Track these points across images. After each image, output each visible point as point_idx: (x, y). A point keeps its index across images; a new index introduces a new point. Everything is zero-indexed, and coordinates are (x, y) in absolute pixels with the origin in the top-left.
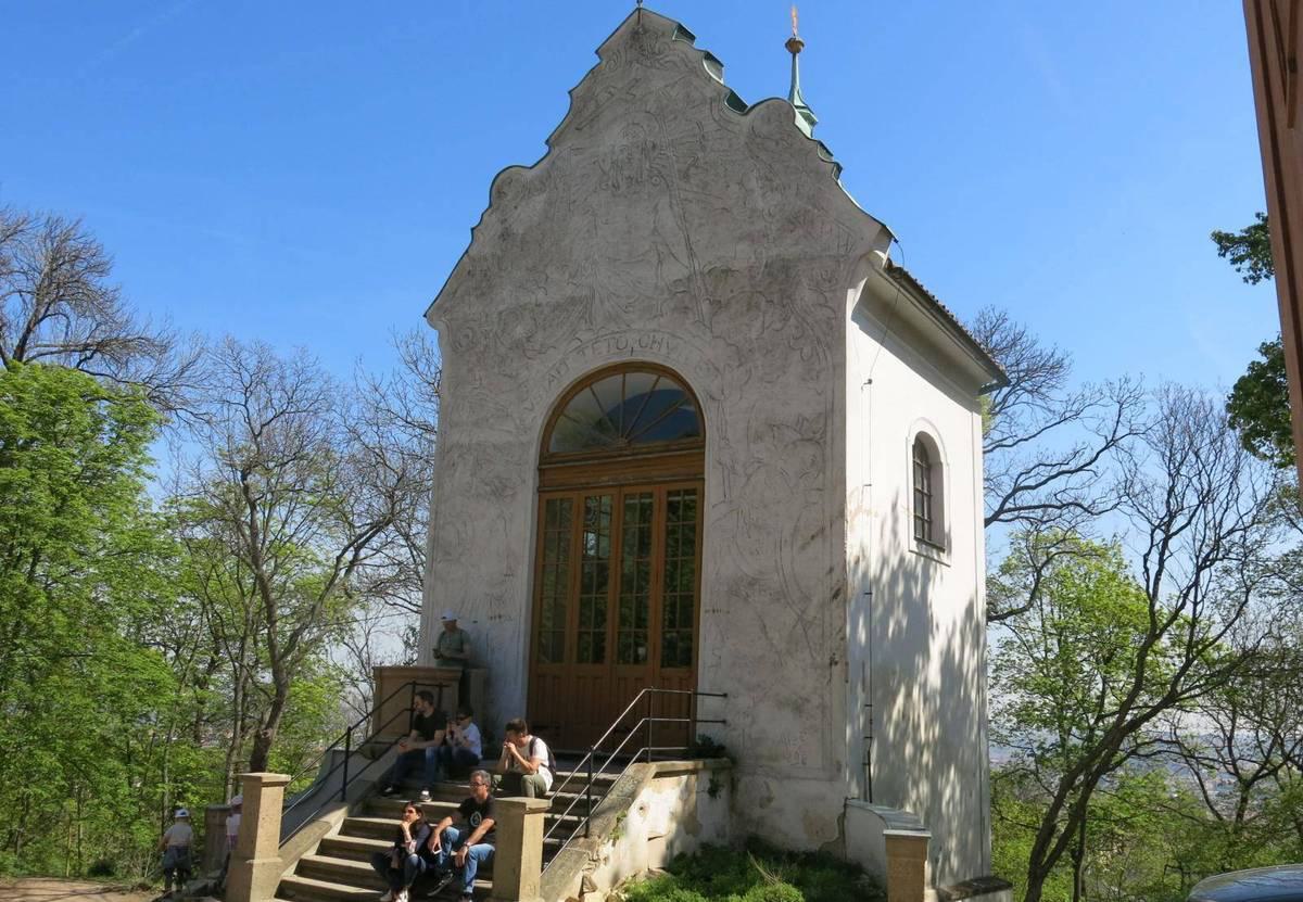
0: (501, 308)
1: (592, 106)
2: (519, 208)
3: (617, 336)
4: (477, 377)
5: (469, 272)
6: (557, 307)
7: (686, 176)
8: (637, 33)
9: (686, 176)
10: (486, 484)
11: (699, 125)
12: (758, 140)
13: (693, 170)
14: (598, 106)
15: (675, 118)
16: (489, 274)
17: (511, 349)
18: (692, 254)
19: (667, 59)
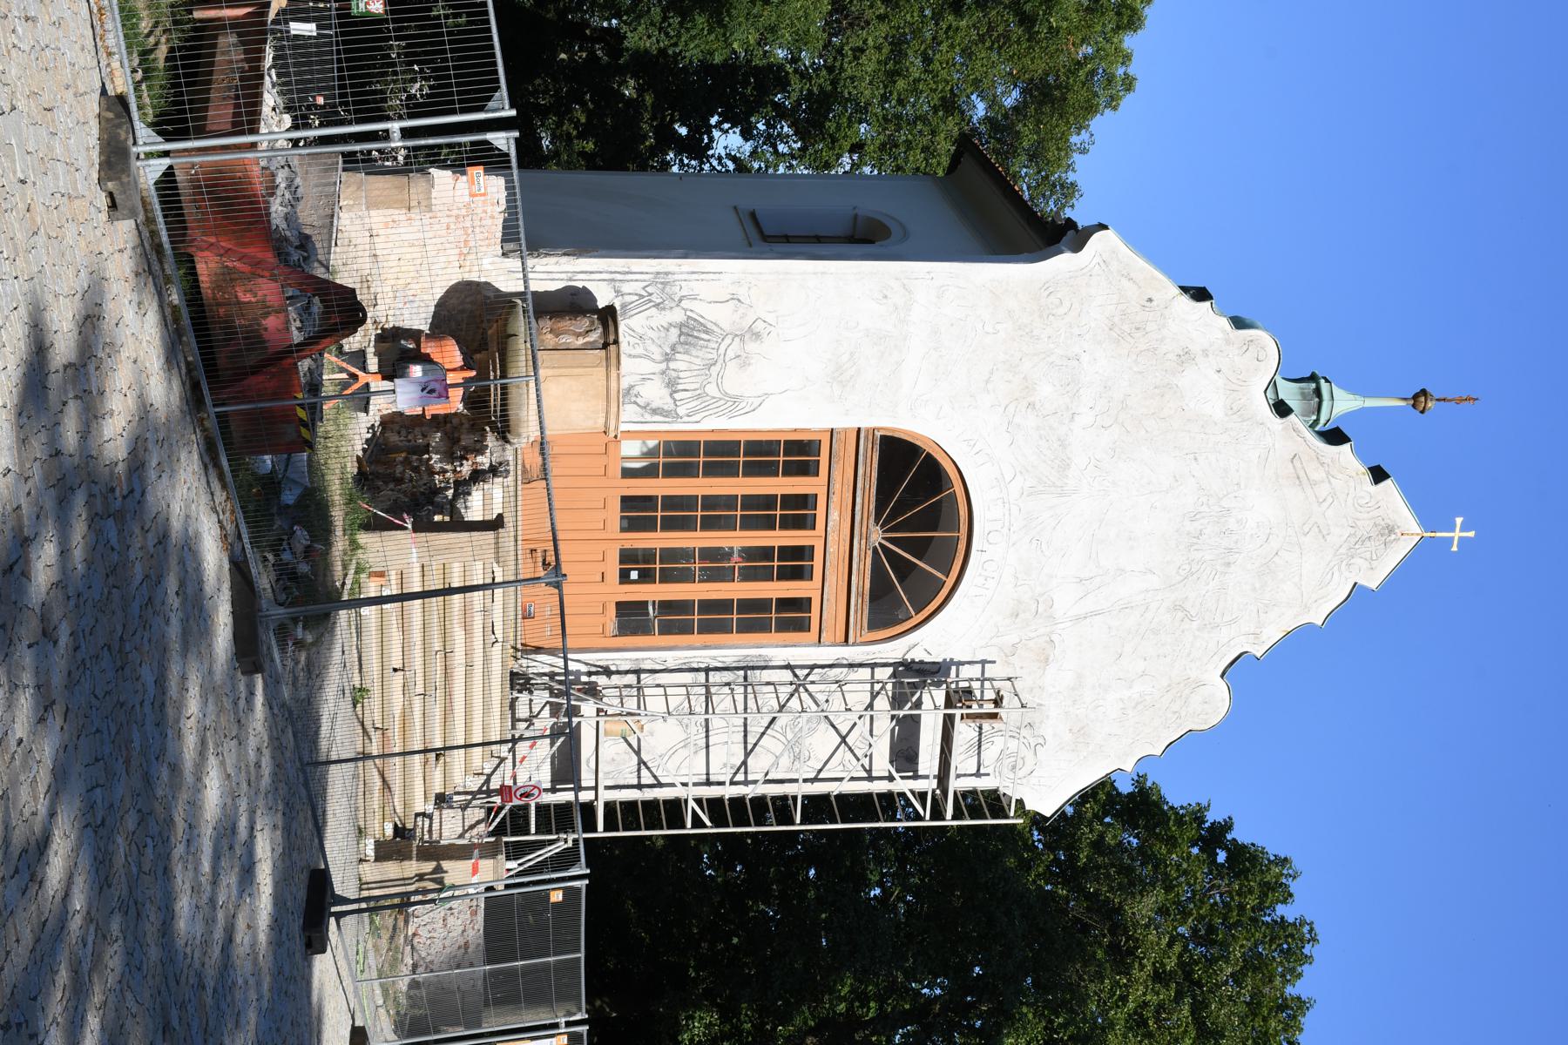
0: (1085, 358)
1: (1317, 474)
2: (1216, 376)
3: (1005, 530)
4: (999, 327)
5: (1150, 300)
6: (1063, 444)
7: (1178, 607)
8: (1391, 531)
9: (1178, 607)
10: (852, 354)
11: (1235, 621)
12: (1187, 691)
13: (1180, 615)
14: (1313, 484)
15: (1254, 589)
16: (1137, 335)
17: (1025, 378)
18: (1079, 619)
19: (1336, 574)
